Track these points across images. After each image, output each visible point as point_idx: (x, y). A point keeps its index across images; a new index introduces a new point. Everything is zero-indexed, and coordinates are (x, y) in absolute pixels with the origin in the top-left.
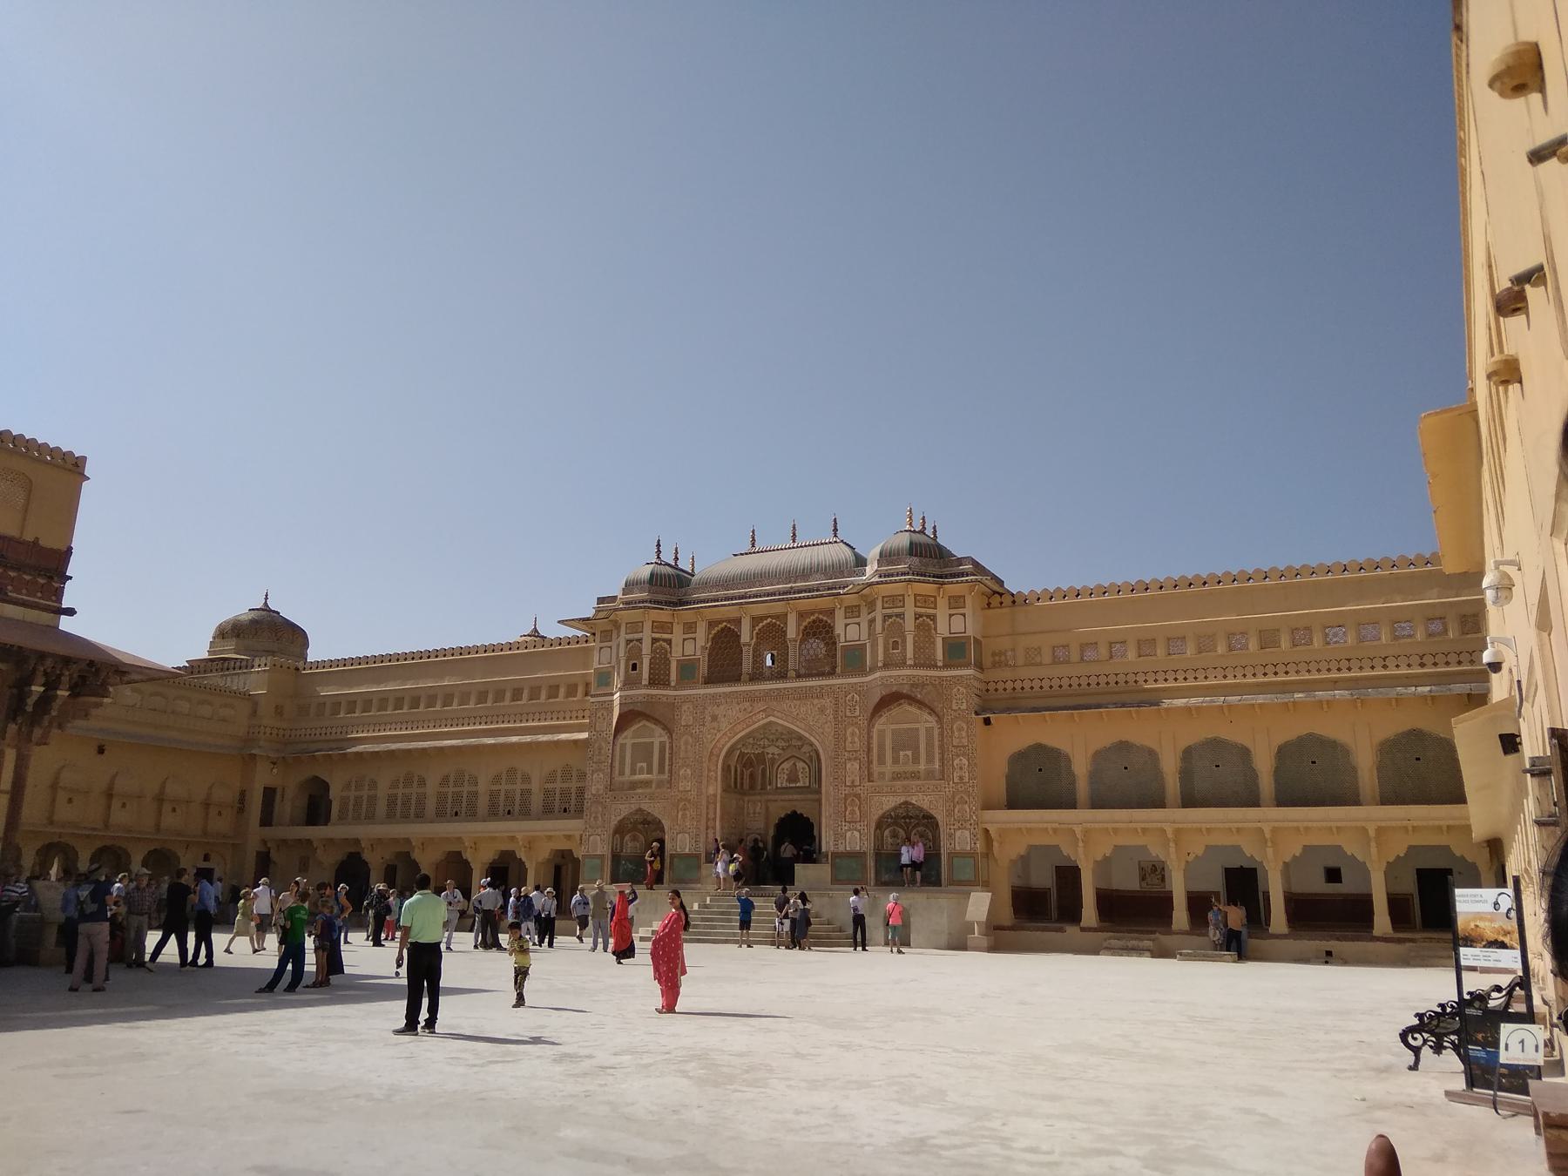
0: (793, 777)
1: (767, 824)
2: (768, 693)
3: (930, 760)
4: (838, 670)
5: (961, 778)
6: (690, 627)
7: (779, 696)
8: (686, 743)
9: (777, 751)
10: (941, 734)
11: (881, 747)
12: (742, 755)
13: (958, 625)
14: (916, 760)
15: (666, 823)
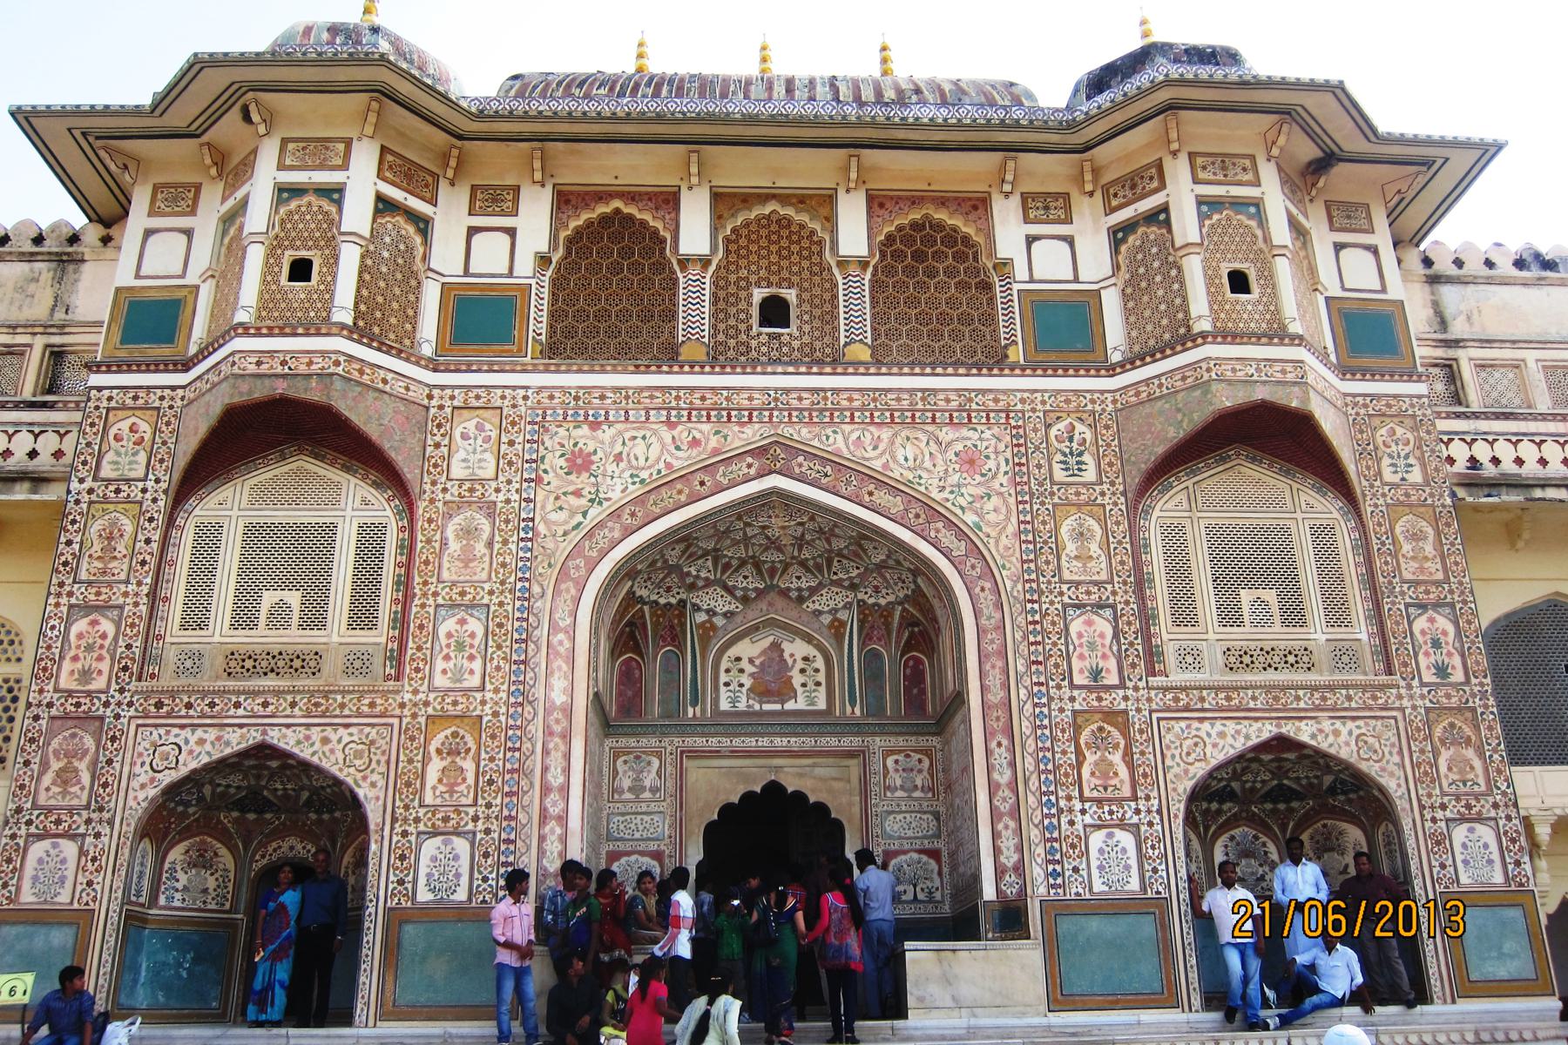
0: (772, 681)
1: (680, 825)
2: (775, 403)
3: (1337, 614)
4: (1016, 354)
5: (1442, 671)
6: (495, 199)
7: (824, 410)
8: (468, 533)
9: (721, 603)
10: (1364, 545)
11: (1179, 572)
12: (631, 598)
13: (1359, 273)
14: (1294, 614)
15: (372, 796)
